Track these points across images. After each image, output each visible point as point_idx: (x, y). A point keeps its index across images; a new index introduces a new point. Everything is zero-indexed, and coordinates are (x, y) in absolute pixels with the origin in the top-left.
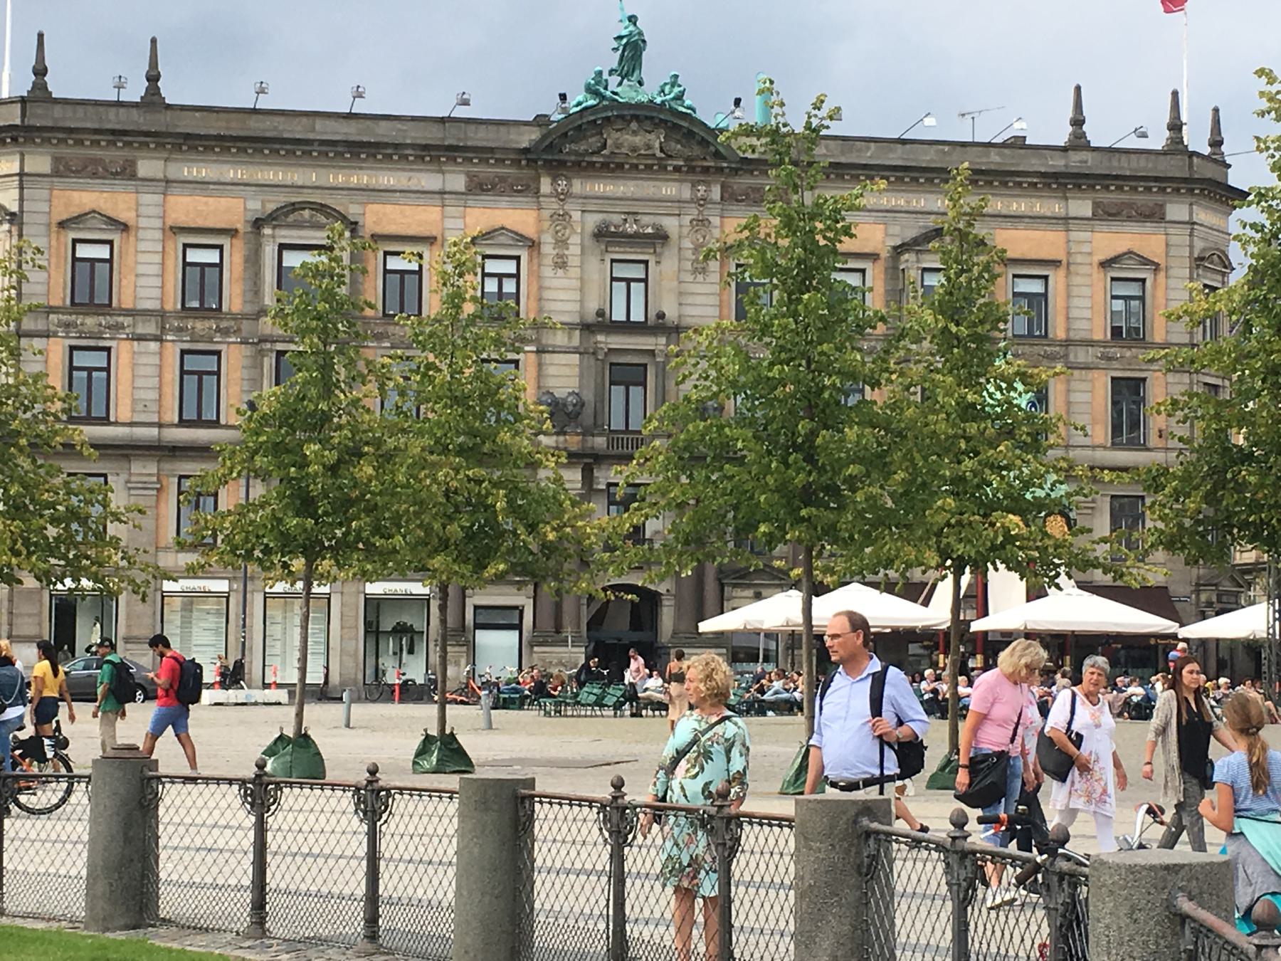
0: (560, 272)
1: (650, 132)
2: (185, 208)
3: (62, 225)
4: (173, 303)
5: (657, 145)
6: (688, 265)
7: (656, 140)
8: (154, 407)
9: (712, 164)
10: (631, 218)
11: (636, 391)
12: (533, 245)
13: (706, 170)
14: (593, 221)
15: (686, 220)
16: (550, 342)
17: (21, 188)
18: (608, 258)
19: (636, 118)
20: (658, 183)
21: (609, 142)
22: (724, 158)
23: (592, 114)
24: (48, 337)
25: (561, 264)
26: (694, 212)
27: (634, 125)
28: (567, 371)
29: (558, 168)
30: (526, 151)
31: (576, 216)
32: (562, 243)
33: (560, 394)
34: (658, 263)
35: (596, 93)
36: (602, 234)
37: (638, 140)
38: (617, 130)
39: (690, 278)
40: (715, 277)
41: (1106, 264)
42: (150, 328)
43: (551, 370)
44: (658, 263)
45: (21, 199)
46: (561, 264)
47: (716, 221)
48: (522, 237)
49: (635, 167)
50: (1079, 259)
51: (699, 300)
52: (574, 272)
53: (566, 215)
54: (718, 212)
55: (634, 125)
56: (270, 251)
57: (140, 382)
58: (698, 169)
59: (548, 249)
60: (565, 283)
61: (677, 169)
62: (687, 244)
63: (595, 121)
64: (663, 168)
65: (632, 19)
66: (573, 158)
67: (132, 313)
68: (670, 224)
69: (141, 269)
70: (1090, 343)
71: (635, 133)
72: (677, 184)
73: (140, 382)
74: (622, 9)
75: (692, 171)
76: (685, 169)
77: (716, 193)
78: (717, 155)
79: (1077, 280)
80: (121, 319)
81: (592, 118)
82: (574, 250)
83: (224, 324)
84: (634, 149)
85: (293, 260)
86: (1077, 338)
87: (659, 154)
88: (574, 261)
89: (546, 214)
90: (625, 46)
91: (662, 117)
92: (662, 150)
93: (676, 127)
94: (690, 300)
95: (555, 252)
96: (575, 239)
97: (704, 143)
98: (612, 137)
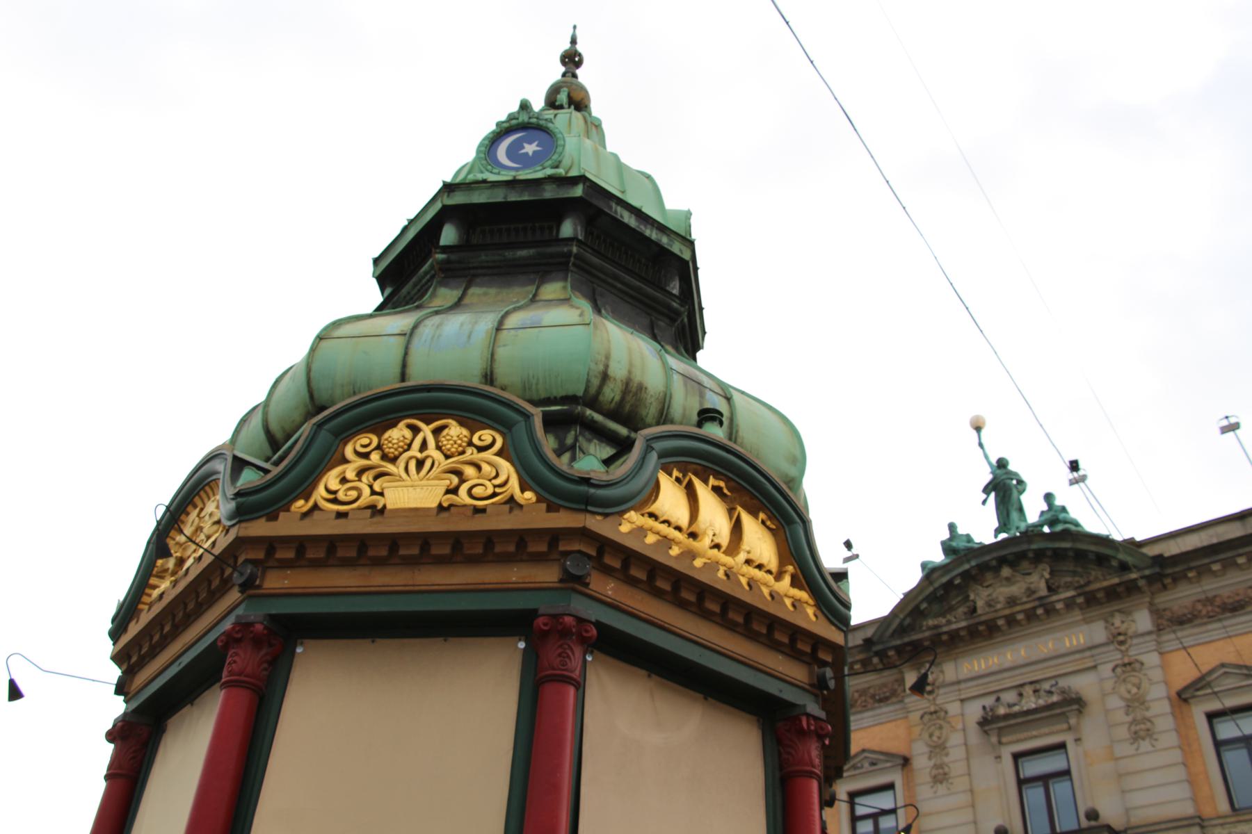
1: (1029, 574)
5: (1043, 585)
6: (1122, 732)
7: (1038, 580)
9: (1116, 580)
12: (906, 761)
13: (1112, 594)
14: (974, 711)
15: (1106, 670)
20: (1057, 635)
21: (980, 603)
23: (942, 576)
25: (940, 777)
26: (1114, 656)
31: (954, 708)
32: (938, 748)
34: (1078, 740)
36: (986, 722)
37: (1016, 589)
40: (1170, 739)
44: (1078, 740)
46: (940, 777)
47: (1152, 659)
48: (889, 755)
49: (1011, 621)
52: (961, 784)
53: (937, 714)
54: (1152, 645)
55: (1006, 571)
58: (1100, 595)
59: (922, 762)
61: (1070, 604)
62: (1115, 702)
63: (950, 582)
64: (1050, 611)
65: (1002, 464)
68: (1083, 684)
72: (1085, 627)
74: (986, 457)
75: (1091, 601)
76: (1080, 600)
77: (1142, 620)
78: (1124, 567)
81: (945, 580)
82: (956, 753)
84: (1012, 601)
88: (957, 767)
89: (915, 717)
91: (1034, 546)
95: (932, 763)
96: (955, 739)
98: (980, 596)
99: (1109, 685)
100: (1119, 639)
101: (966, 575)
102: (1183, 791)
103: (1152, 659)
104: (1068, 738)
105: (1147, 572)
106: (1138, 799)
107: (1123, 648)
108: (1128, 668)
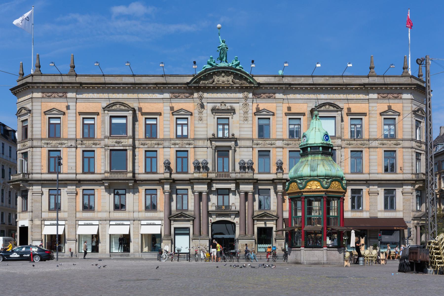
0: (200, 122)
1: (228, 76)
2: (83, 107)
3: (45, 113)
4: (80, 136)
5: (231, 80)
6: (242, 119)
7: (230, 78)
8: (74, 168)
9: (249, 85)
10: (223, 104)
11: (226, 159)
15: (241, 104)
16: (197, 144)
17: (32, 102)
18: (216, 117)
19: (223, 72)
21: (215, 80)
22: (253, 83)
24: (41, 147)
26: (243, 101)
27: (223, 74)
28: (202, 153)
29: (199, 89)
30: (188, 83)
33: (200, 161)
35: (211, 65)
37: (225, 79)
38: (218, 76)
39: (243, 123)
40: (250, 122)
41: (381, 114)
42: (73, 143)
43: (198, 153)
45: (32, 106)
50: (373, 112)
51: (246, 129)
52: (205, 122)
56: (107, 119)
57: (70, 161)
60: (202, 126)
66: (203, 85)
67: (67, 139)
68: (236, 106)
69: (69, 126)
70: (376, 140)
71: (223, 77)
73: (70, 161)
78: (250, 83)
79: (372, 119)
80: (63, 141)
82: (204, 115)
83: (95, 142)
84: (223, 82)
85: (114, 121)
86: (372, 138)
87: (231, 83)
88: (204, 118)
90: (221, 49)
92: (232, 81)
93: (237, 74)
94: (242, 129)
95: (199, 116)
97: (246, 79)
98: (216, 78)
99: (241, 107)
100: (246, 98)
101: (214, 73)
102: (251, 133)
103: (251, 104)
104: (230, 117)
105: (255, 85)
106: (242, 133)
107: (246, 100)
108: (245, 105)
